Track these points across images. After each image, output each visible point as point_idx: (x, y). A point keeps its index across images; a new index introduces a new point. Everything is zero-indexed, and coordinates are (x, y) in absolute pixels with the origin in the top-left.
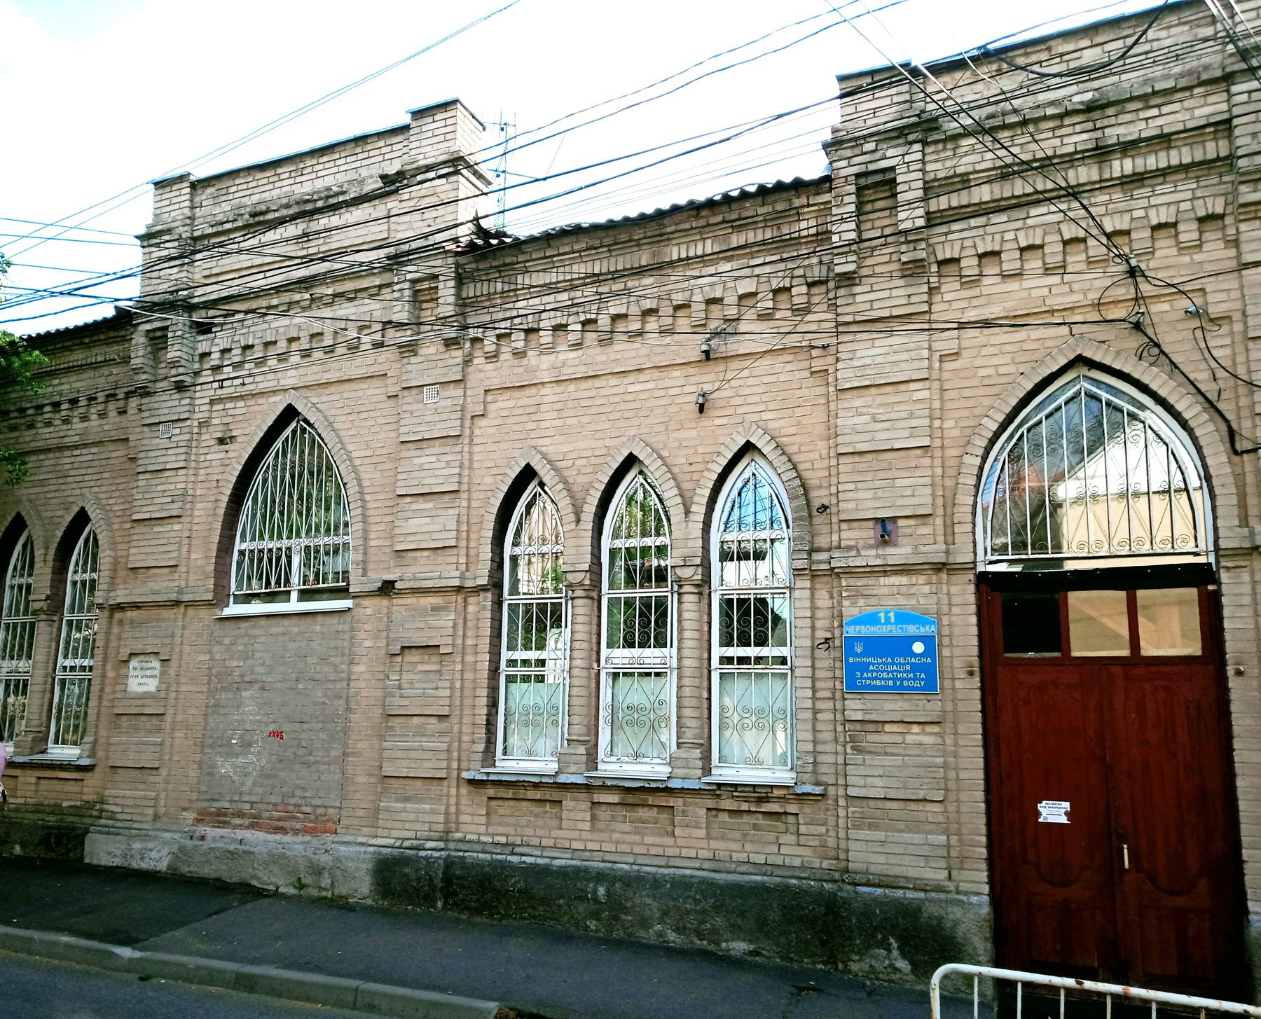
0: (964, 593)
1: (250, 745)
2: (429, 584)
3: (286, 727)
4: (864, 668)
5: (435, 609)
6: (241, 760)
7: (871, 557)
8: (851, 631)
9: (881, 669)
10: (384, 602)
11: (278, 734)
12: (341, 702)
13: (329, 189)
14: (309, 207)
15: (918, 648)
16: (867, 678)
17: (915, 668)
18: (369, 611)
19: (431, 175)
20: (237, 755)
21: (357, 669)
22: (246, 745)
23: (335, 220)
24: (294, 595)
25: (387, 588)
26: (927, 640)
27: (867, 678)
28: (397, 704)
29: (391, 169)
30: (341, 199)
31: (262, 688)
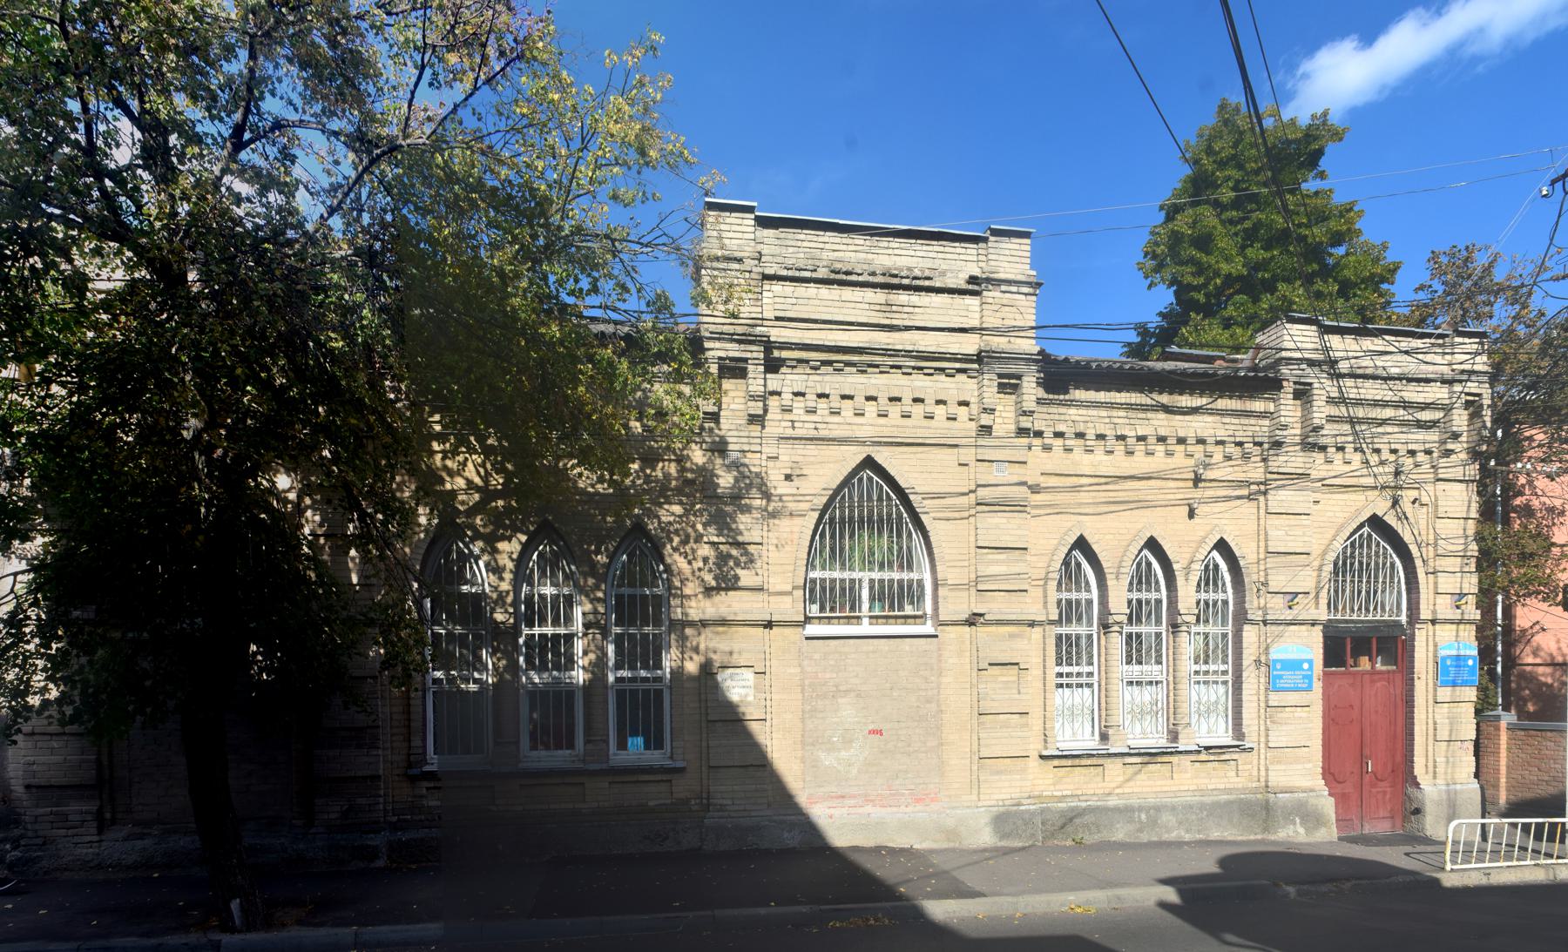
0: (1317, 635)
1: (851, 741)
2: (1014, 617)
3: (884, 727)
4: (1280, 677)
5: (1012, 636)
6: (843, 754)
7: (1288, 615)
8: (1273, 655)
9: (1289, 678)
10: (967, 629)
11: (880, 732)
12: (934, 705)
13: (909, 269)
14: (895, 281)
15: (1306, 666)
16: (1280, 684)
17: (1305, 677)
18: (952, 636)
19: (1014, 289)
20: (839, 750)
21: (944, 680)
22: (848, 742)
23: (915, 298)
24: (866, 621)
25: (973, 620)
26: (1310, 662)
27: (1280, 684)
28: (987, 706)
29: (976, 272)
30: (927, 283)
31: (858, 696)
